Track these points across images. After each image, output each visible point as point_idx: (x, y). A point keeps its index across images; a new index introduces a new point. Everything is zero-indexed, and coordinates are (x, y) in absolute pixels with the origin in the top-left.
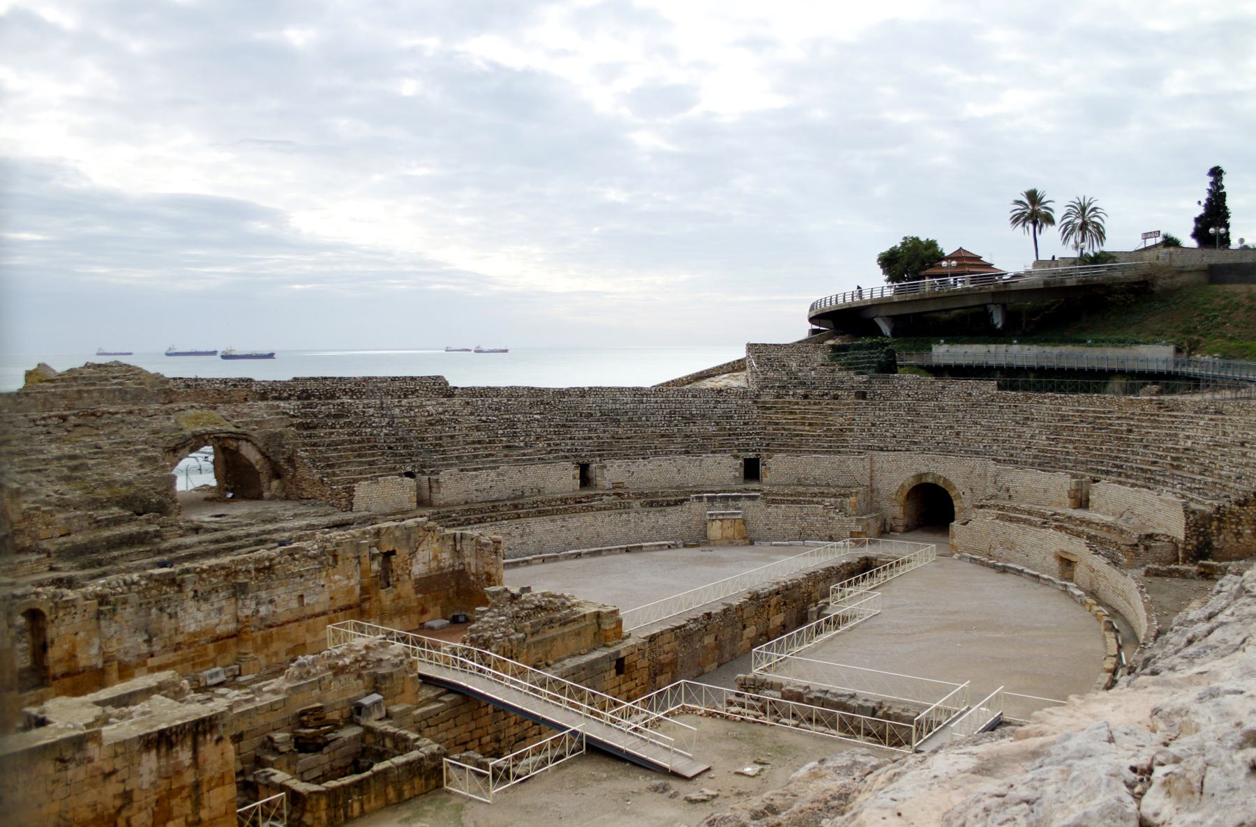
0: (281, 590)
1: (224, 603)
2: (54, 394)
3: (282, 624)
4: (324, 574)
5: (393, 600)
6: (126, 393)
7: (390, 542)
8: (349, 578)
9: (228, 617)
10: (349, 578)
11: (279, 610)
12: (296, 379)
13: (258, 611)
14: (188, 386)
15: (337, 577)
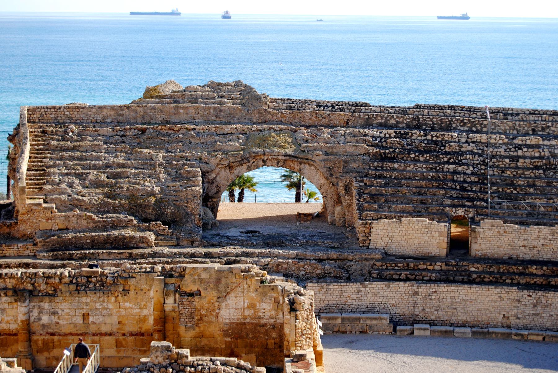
0: (65, 306)
1: (6, 306)
2: (154, 108)
3: (66, 335)
4: (113, 299)
5: (195, 338)
6: (221, 111)
7: (194, 282)
8: (141, 308)
9: (9, 318)
10: (141, 308)
11: (61, 322)
12: (418, 106)
13: (40, 319)
14: (291, 108)
15: (127, 305)
